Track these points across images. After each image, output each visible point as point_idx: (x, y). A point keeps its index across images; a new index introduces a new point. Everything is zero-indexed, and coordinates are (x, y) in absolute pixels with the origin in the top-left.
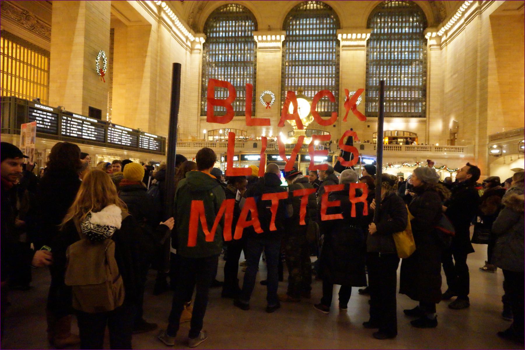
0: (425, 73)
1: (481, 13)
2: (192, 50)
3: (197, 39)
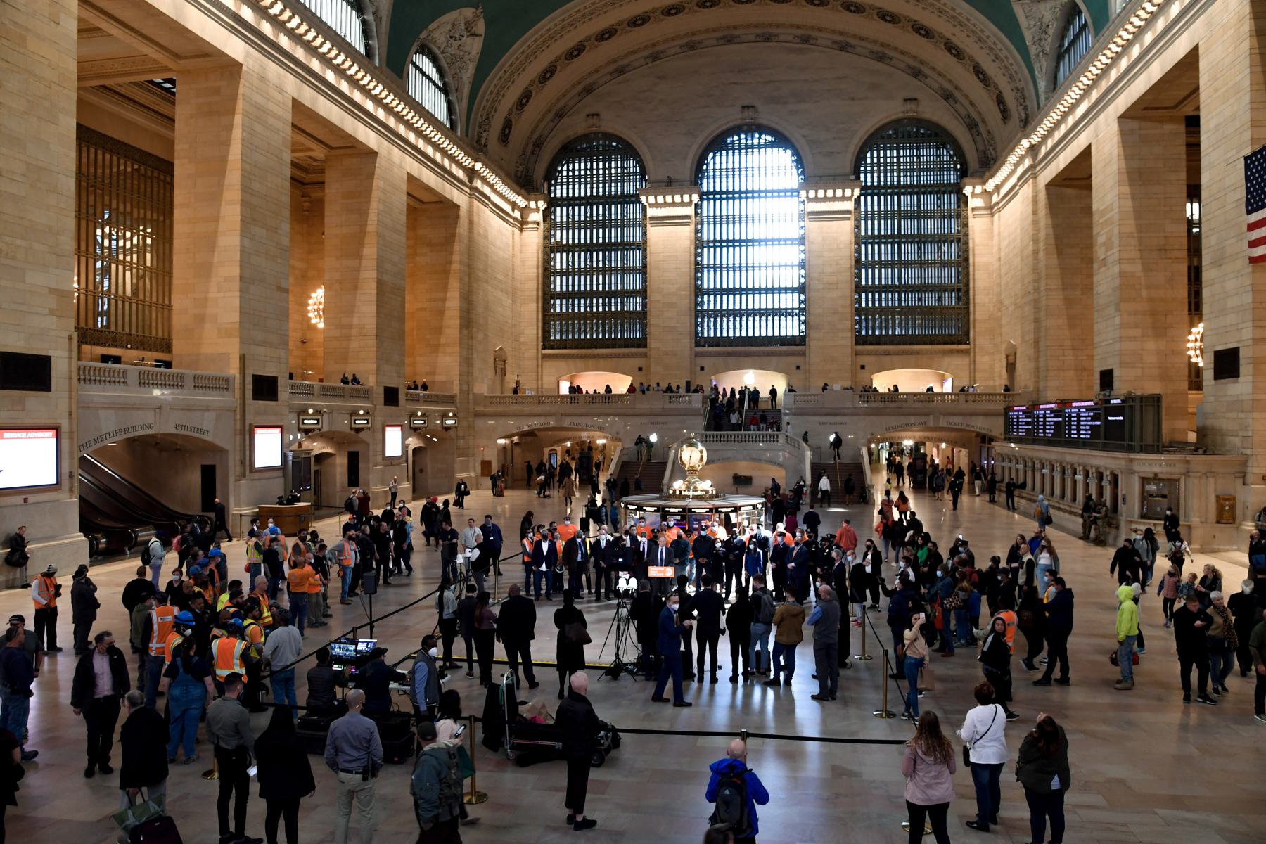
0: (963, 262)
1: (1035, 177)
2: (522, 224)
3: (532, 205)
